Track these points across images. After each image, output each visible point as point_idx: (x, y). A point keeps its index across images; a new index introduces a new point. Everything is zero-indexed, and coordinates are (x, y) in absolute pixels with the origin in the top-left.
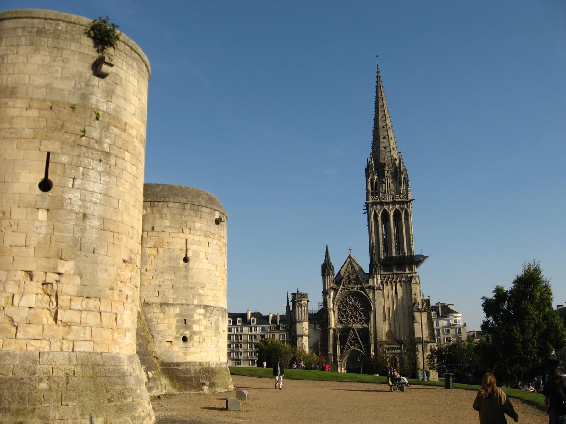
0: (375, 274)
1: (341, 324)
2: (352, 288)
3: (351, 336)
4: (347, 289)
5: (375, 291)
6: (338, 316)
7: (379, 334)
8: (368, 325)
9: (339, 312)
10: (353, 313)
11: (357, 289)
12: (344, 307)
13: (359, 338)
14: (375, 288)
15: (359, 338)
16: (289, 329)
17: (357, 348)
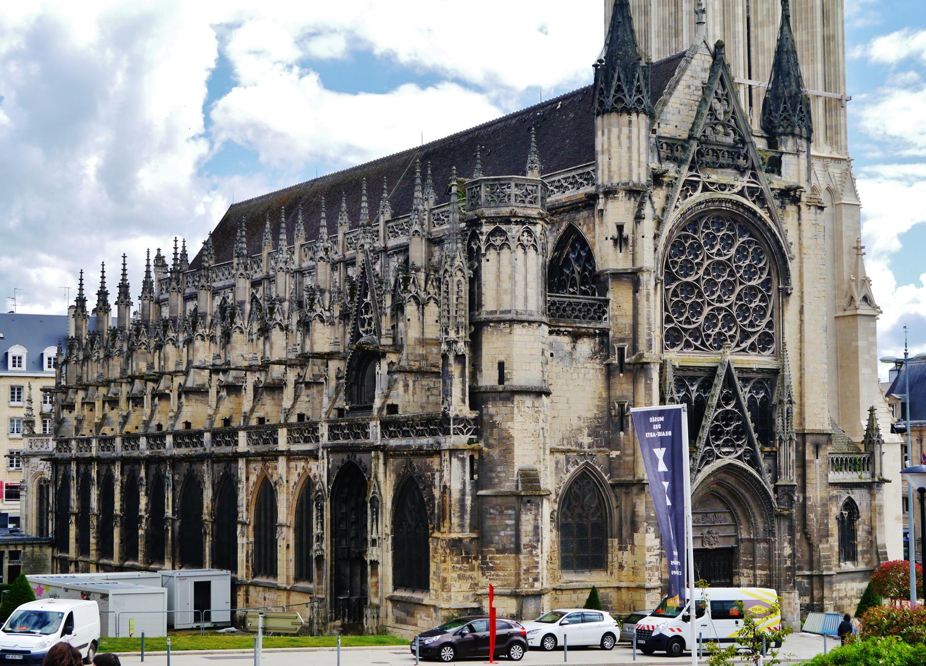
0: (801, 137)
1: (673, 345)
2: (723, 187)
3: (719, 406)
4: (705, 189)
5: (804, 208)
6: (667, 310)
7: (809, 401)
8: (780, 354)
9: (667, 290)
10: (720, 300)
11: (741, 193)
12: (688, 268)
13: (748, 414)
14: (804, 198)
15: (748, 414)
16: (463, 356)
17: (739, 458)
